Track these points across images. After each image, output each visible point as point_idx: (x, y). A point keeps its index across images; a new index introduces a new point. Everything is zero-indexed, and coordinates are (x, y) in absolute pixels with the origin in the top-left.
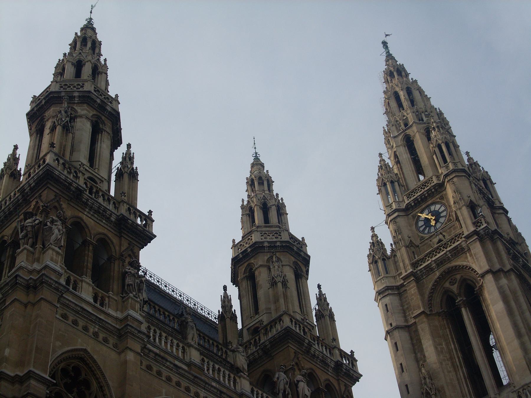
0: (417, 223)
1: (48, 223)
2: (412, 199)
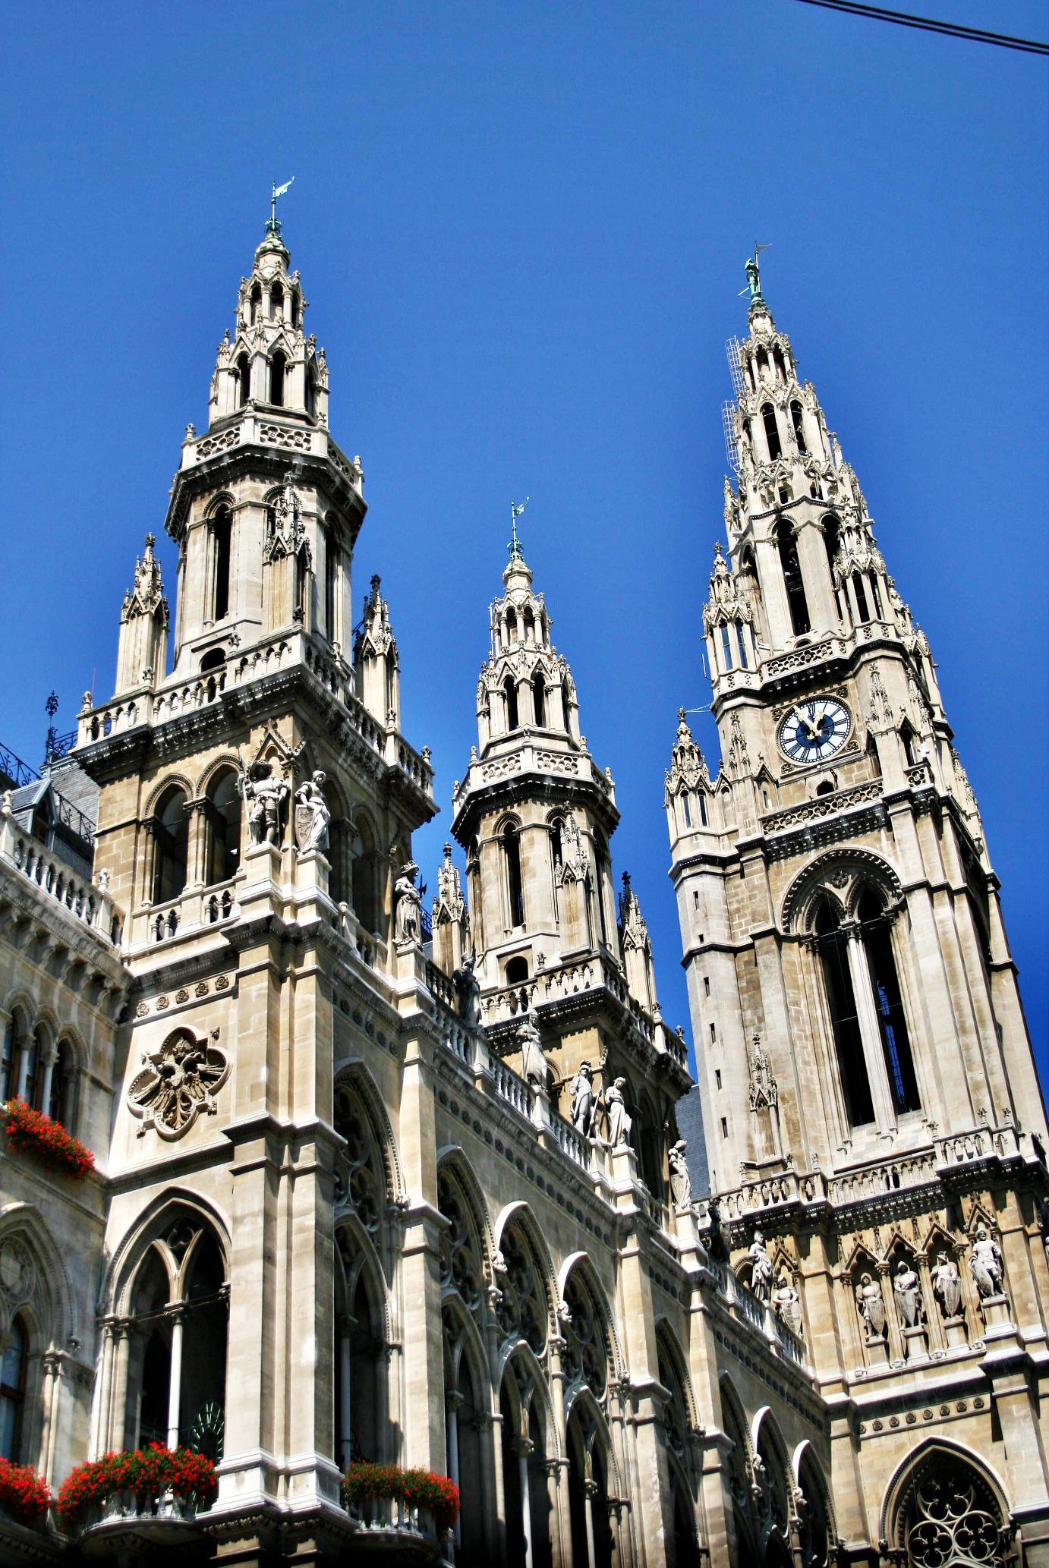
0: (780, 730)
1: (303, 798)
2: (780, 675)
